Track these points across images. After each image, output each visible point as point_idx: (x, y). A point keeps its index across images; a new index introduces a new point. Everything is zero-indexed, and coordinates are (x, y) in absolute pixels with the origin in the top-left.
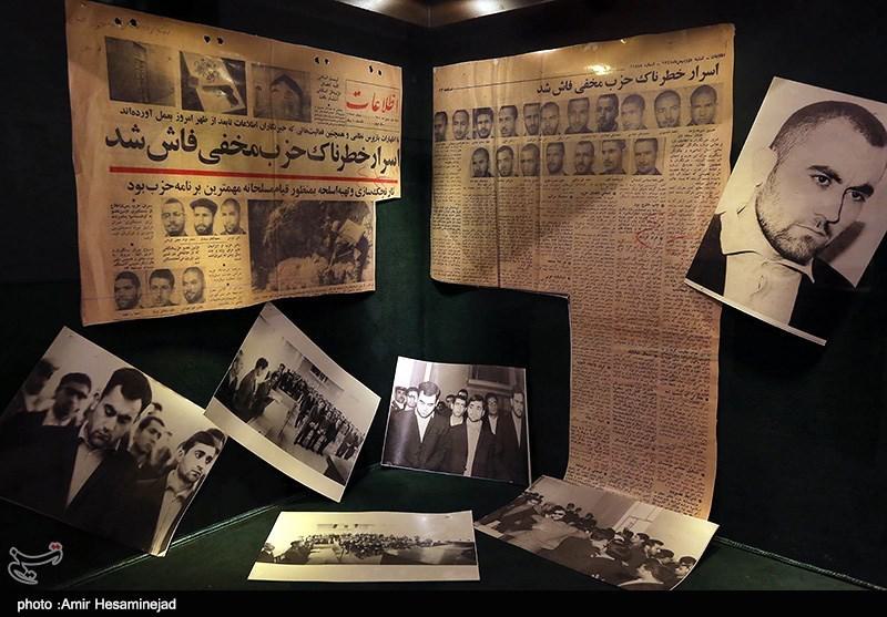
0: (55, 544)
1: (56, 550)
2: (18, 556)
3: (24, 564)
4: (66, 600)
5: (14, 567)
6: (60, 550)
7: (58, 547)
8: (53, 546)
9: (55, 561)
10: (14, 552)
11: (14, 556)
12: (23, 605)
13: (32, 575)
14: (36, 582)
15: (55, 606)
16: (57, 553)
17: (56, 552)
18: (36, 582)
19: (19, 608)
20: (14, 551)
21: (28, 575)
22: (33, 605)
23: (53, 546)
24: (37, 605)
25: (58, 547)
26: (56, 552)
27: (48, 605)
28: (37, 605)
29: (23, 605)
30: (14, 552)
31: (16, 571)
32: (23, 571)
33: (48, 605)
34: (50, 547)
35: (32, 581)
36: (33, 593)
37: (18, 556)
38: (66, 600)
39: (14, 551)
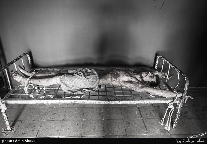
1: (13, 128)
2: (4, 130)
3: (4, 131)
4: (16, 140)
5: (3, 132)
7: (13, 128)
10: (3, 129)
13: (7, 134)
15: (13, 141)
16: (14, 129)
19: (3, 142)
21: (6, 134)
25: (13, 128)
27: (11, 141)
30: (3, 129)
31: (4, 133)
32: (5, 133)
33: (11, 141)
37: (4, 130)
38: (16, 140)
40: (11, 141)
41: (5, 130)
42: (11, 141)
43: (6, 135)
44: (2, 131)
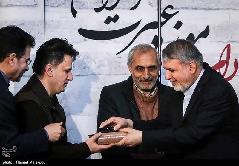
0: (15, 146)
1: (15, 148)
2: (5, 150)
5: (3, 153)
6: (16, 148)
7: (15, 147)
8: (14, 147)
9: (15, 151)
10: (3, 148)
11: (4, 150)
12: (4, 163)
14: (9, 157)
15: (13, 163)
16: (15, 149)
17: (15, 149)
18: (9, 157)
19: (3, 163)
20: (3, 148)
21: (7, 155)
22: (7, 163)
23: (14, 147)
24: (8, 163)
25: (15, 147)
26: (15, 149)
27: (11, 163)
28: (8, 163)
29: (4, 163)
30: (3, 148)
31: (4, 154)
32: (6, 154)
33: (11, 163)
34: (13, 147)
35: (8, 156)
36: (7, 159)
37: (5, 150)
39: (3, 148)
40: (10, 162)
41: (6, 150)
42: (10, 162)
43: (6, 155)
44: (2, 151)
